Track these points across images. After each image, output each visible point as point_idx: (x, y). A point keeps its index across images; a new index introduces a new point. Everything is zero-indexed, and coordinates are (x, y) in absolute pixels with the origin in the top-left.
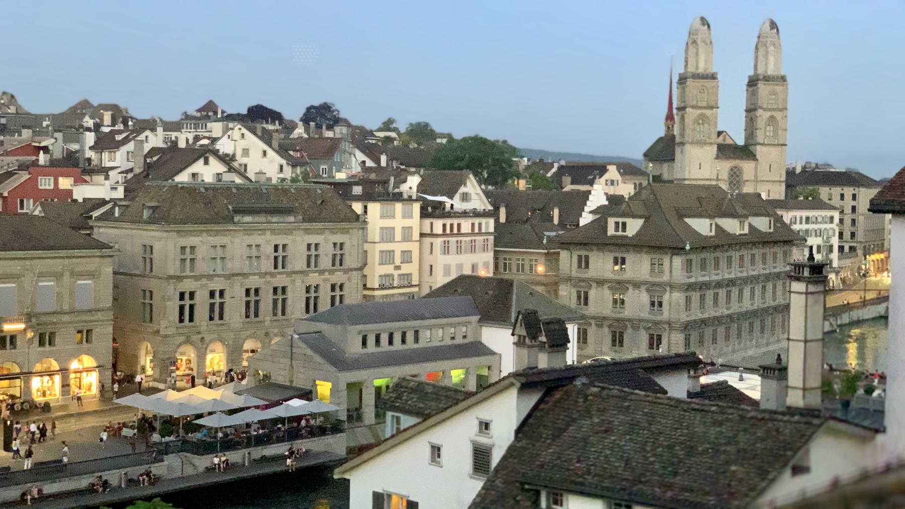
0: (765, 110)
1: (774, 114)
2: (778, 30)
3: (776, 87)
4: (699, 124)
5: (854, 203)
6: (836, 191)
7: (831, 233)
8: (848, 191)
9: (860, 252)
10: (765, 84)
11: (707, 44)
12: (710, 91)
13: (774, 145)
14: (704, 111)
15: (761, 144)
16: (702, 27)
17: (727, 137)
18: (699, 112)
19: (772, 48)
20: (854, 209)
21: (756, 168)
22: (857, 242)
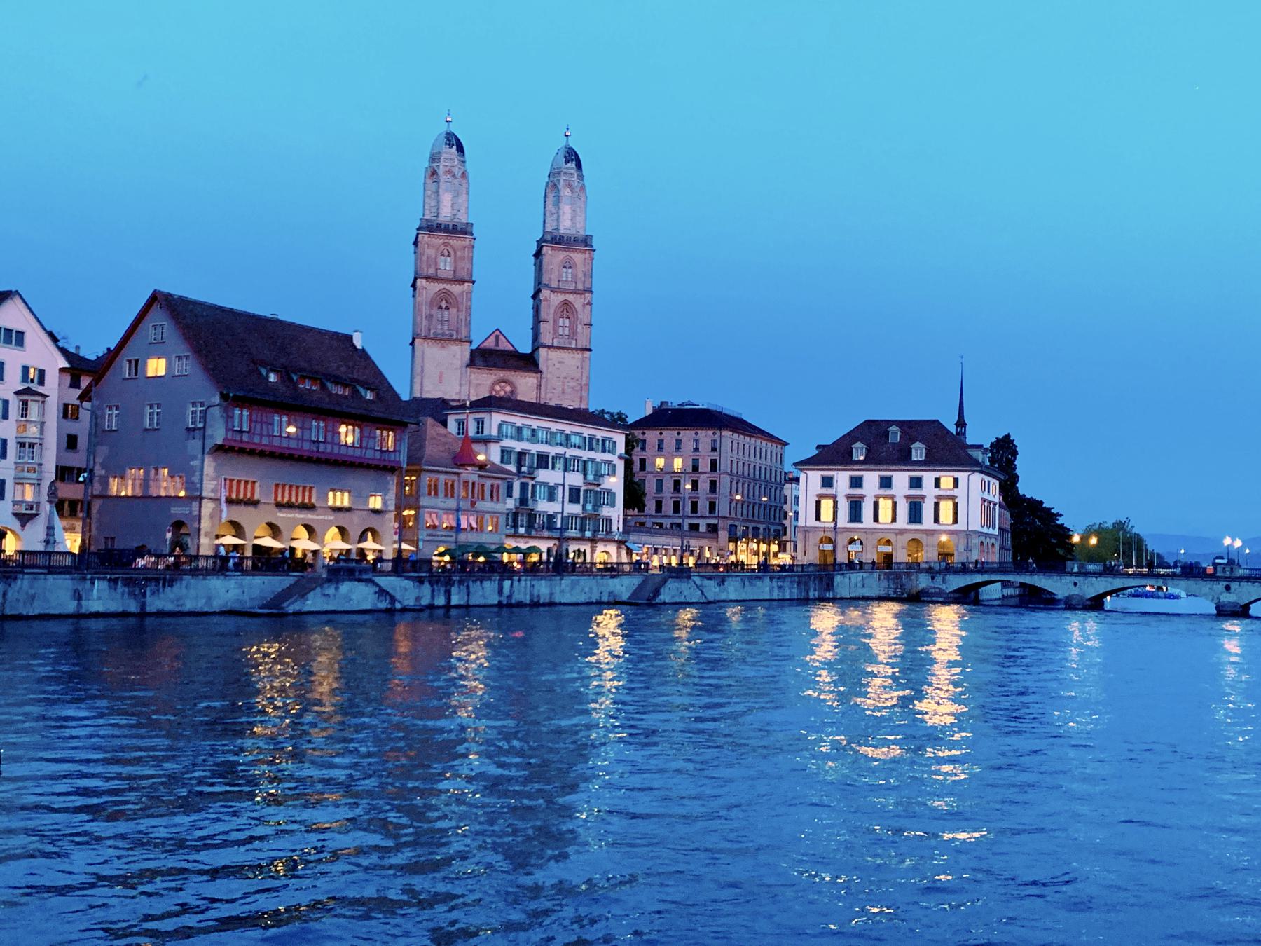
0: (553, 291)
1: (570, 298)
2: (579, 166)
3: (572, 255)
4: (440, 307)
5: (715, 456)
6: (687, 435)
7: (605, 469)
8: (706, 436)
9: (723, 535)
10: (553, 248)
11: (454, 176)
12: (459, 254)
13: (572, 349)
14: (448, 286)
15: (549, 347)
16: (446, 149)
17: (501, 337)
18: (440, 286)
19: (567, 192)
20: (714, 464)
21: (539, 386)
22: (718, 518)
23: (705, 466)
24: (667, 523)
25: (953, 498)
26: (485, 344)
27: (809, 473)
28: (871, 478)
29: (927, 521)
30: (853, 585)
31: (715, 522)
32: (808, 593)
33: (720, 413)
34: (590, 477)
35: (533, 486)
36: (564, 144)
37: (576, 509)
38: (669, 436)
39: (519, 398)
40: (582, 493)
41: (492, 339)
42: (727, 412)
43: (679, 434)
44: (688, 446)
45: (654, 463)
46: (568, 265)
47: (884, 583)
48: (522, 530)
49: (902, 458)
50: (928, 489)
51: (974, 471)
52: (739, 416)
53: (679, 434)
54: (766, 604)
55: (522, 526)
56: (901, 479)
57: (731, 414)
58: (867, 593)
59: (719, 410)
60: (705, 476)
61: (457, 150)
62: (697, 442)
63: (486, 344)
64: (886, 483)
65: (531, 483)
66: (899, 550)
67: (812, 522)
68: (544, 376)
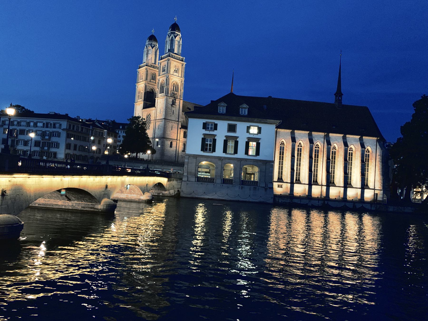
37: (37, 149)
40: (41, 143)
61: (149, 40)
65: (16, 139)
68: (156, 108)
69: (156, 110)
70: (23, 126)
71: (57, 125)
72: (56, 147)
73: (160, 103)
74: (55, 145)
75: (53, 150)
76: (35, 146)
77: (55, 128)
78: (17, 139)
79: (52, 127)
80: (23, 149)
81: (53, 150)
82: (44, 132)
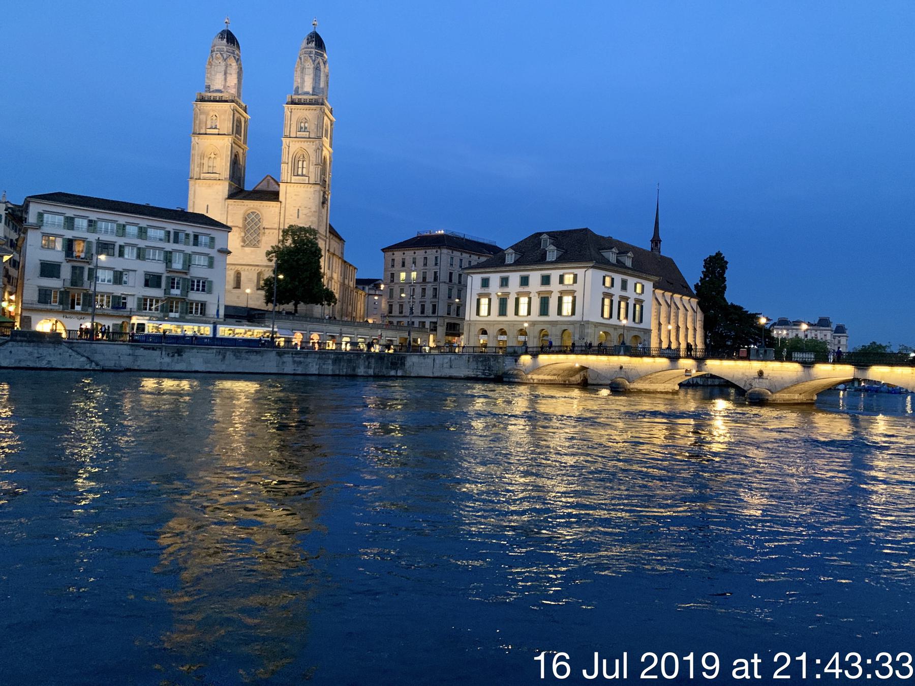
6: (420, 254)
23: (430, 278)
24: (405, 321)
25: (572, 292)
26: (259, 187)
27: (474, 276)
28: (514, 278)
29: (553, 315)
30: (437, 366)
31: (434, 320)
32: (354, 369)
33: (463, 239)
34: (178, 265)
35: (91, 271)
36: (312, 30)
38: (409, 254)
39: (189, 211)
41: (265, 182)
42: (468, 238)
43: (415, 253)
44: (420, 262)
45: (399, 276)
46: (305, 120)
47: (473, 365)
48: (78, 308)
49: (540, 260)
50: (555, 286)
51: (588, 268)
52: (493, 244)
53: (415, 253)
54: (273, 377)
55: (78, 304)
56: (535, 277)
57: (476, 240)
58: (454, 373)
59: (462, 236)
60: (430, 284)
61: (228, 42)
62: (426, 258)
63: (260, 188)
64: (525, 281)
66: (531, 339)
67: (474, 317)
68: (283, 205)
69: (283, 209)
70: (155, 239)
71: (203, 239)
72: (203, 290)
73: (296, 195)
74: (198, 286)
75: (195, 296)
76: (147, 284)
77: (197, 245)
78: (91, 266)
79: (191, 243)
80: (112, 292)
81: (195, 296)
82: (167, 252)
